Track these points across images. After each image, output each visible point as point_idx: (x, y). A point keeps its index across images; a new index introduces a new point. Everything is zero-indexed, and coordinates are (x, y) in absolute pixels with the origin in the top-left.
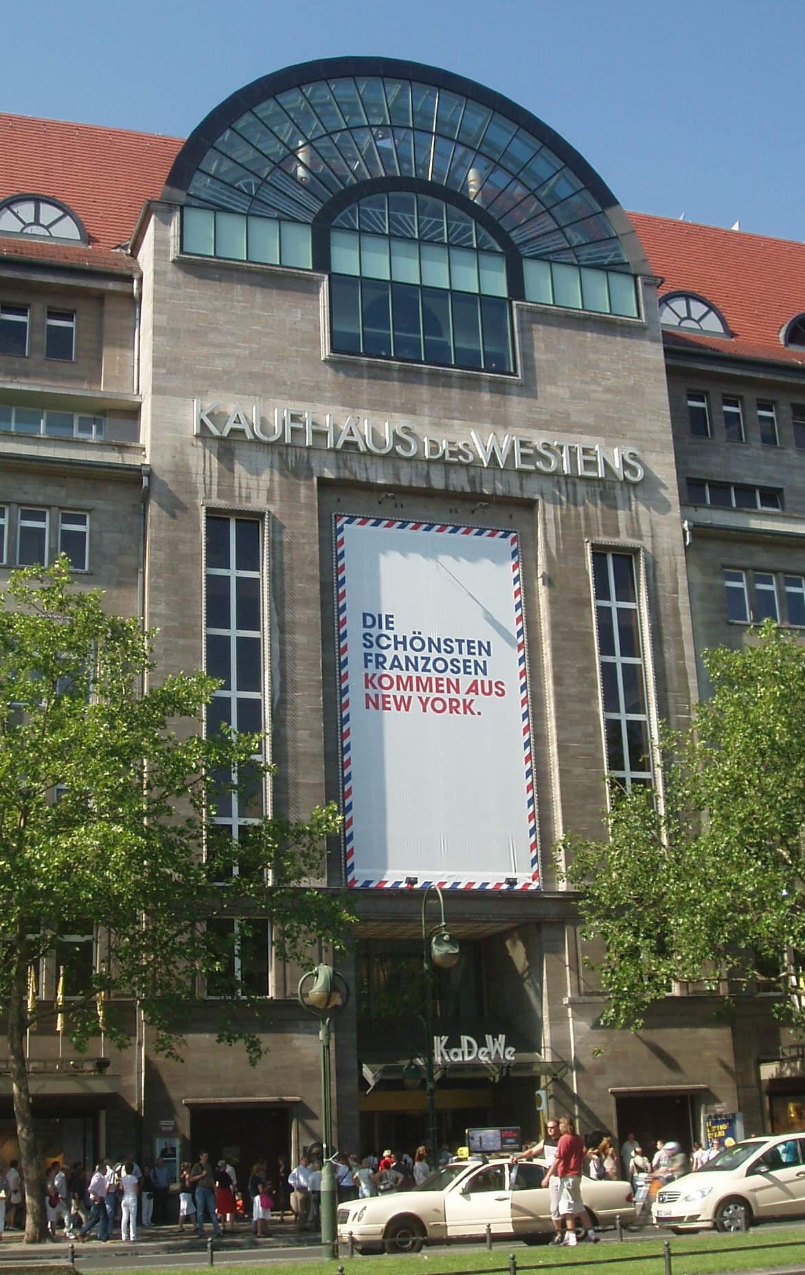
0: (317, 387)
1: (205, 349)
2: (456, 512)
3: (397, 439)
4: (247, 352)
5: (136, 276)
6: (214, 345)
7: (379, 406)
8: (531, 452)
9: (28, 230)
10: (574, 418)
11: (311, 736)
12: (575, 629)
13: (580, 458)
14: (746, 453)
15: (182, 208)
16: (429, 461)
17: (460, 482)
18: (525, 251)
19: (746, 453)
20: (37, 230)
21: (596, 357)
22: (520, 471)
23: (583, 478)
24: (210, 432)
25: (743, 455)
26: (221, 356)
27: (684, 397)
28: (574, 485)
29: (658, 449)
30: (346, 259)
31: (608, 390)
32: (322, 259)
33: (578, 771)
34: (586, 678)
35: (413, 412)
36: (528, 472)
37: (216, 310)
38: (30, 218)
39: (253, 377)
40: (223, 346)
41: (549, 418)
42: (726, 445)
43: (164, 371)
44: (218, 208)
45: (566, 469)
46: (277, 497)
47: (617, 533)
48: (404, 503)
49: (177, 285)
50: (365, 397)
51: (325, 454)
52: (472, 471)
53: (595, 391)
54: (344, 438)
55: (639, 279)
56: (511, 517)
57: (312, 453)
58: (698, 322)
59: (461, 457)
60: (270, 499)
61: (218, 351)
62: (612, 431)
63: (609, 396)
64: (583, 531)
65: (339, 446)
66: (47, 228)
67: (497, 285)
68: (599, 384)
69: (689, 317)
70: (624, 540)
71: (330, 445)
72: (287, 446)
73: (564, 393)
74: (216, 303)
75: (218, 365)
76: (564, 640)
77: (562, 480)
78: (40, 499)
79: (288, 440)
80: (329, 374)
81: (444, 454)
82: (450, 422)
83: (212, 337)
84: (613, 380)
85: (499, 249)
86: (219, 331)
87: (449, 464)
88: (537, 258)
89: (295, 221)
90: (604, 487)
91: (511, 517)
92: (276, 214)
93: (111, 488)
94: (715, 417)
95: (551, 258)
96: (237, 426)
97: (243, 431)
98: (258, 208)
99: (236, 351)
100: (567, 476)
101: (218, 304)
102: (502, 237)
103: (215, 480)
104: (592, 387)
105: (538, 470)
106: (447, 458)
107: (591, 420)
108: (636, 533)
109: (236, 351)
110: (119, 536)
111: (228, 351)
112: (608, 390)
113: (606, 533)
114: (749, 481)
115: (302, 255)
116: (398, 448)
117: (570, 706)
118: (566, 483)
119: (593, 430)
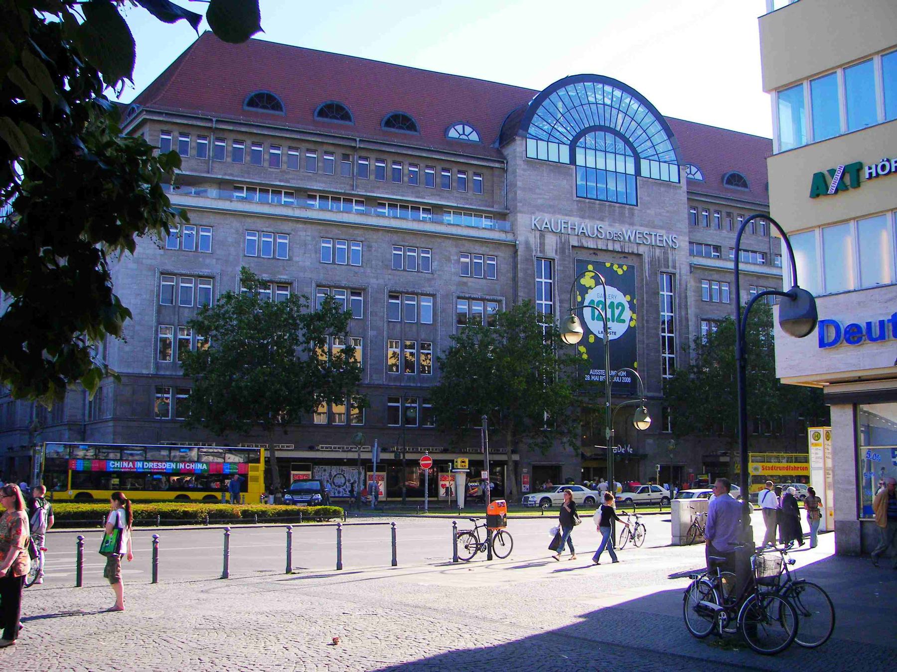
0: (571, 211)
5: (505, 162)
6: (538, 194)
7: (592, 218)
8: (641, 236)
9: (461, 137)
10: (656, 223)
13: (658, 238)
16: (608, 239)
18: (641, 155)
28: (655, 249)
35: (602, 220)
36: (640, 244)
38: (461, 132)
39: (551, 206)
44: (537, 139)
45: (653, 244)
46: (558, 253)
49: (524, 170)
50: (587, 214)
54: (581, 231)
58: (694, 175)
60: (556, 254)
61: (539, 196)
63: (668, 214)
66: (467, 136)
67: (631, 170)
69: (690, 173)
70: (670, 270)
75: (540, 202)
82: (614, 224)
83: (537, 191)
88: (644, 158)
89: (564, 144)
92: (557, 141)
94: (699, 217)
95: (650, 158)
96: (546, 226)
98: (551, 139)
102: (633, 149)
103: (539, 246)
107: (661, 224)
108: (674, 267)
112: (668, 212)
113: (665, 267)
114: (709, 243)
115: (565, 158)
116: (599, 235)
119: (662, 228)
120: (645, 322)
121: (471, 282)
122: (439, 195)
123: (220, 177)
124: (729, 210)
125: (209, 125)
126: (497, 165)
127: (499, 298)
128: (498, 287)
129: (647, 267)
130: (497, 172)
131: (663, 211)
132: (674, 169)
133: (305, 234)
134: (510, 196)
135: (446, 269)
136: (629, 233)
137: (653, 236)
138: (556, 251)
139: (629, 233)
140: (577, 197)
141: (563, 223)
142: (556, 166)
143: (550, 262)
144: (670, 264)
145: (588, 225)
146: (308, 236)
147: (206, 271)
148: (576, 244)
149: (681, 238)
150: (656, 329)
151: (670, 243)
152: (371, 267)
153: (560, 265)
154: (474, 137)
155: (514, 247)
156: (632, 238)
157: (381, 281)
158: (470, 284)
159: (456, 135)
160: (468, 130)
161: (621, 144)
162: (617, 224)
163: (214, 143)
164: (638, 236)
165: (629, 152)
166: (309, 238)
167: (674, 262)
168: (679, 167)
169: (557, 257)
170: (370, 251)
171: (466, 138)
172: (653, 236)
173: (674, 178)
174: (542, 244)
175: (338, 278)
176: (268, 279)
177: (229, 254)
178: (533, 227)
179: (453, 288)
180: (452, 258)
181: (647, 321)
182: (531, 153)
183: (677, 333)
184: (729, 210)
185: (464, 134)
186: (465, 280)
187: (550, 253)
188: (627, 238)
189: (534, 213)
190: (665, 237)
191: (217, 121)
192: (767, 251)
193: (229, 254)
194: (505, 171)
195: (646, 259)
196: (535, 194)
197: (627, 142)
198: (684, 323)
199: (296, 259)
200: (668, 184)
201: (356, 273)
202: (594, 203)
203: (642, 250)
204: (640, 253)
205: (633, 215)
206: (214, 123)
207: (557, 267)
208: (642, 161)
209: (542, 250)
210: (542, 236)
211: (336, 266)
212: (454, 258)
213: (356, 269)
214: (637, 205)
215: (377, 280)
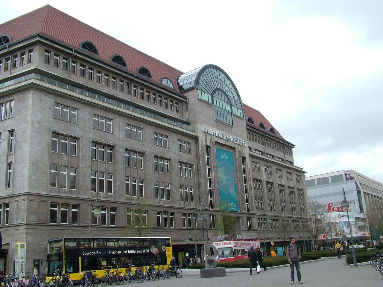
7: (220, 129)
17: (228, 144)
20: (167, 84)
31: (241, 130)
33: (242, 193)
35: (223, 131)
37: (202, 109)
38: (167, 83)
44: (202, 90)
47: (243, 154)
54: (218, 135)
57: (214, 137)
62: (242, 138)
63: (241, 131)
66: (169, 84)
70: (244, 156)
75: (204, 119)
80: (215, 123)
87: (227, 140)
92: (207, 92)
93: (192, 139)
95: (234, 106)
99: (205, 117)
102: (230, 101)
119: (240, 137)
120: (239, 178)
122: (164, 110)
123: (77, 82)
125: (71, 52)
126: (184, 100)
127: (193, 164)
129: (237, 153)
130: (184, 104)
132: (241, 112)
133: (119, 121)
134: (191, 115)
135: (174, 147)
142: (208, 103)
143: (208, 147)
144: (244, 153)
145: (219, 133)
146: (120, 121)
147: (75, 135)
148: (216, 141)
149: (246, 142)
152: (146, 142)
153: (213, 149)
154: (171, 86)
155: (196, 139)
157: (150, 150)
158: (182, 155)
159: (165, 84)
160: (169, 82)
161: (226, 98)
162: (227, 133)
163: (71, 63)
164: (234, 139)
165: (229, 102)
166: (121, 123)
167: (245, 152)
168: (243, 111)
169: (211, 146)
170: (145, 133)
171: (168, 85)
173: (242, 116)
174: (206, 139)
175: (133, 146)
176: (104, 143)
177: (86, 126)
178: (203, 131)
179: (177, 157)
180: (175, 142)
182: (200, 97)
183: (248, 184)
185: (168, 83)
186: (180, 153)
187: (209, 144)
189: (202, 124)
191: (75, 51)
192: (263, 151)
193: (86, 126)
194: (187, 103)
195: (236, 149)
197: (228, 98)
198: (250, 180)
199: (116, 133)
200: (240, 118)
201: (141, 144)
202: (220, 123)
203: (235, 146)
204: (235, 147)
205: (232, 130)
206: (74, 51)
208: (233, 107)
209: (206, 142)
210: (206, 136)
211: (132, 140)
212: (176, 142)
213: (141, 142)
214: (233, 126)
215: (149, 149)
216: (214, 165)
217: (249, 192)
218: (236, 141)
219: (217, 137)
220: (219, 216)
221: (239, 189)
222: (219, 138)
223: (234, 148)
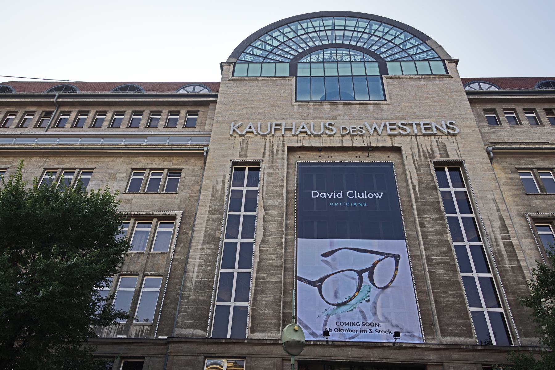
1: (239, 106)
2: (359, 157)
3: (326, 128)
4: (258, 106)
10: (418, 113)
11: (276, 257)
12: (429, 200)
13: (423, 127)
14: (522, 130)
15: (235, 63)
16: (343, 136)
17: (358, 142)
19: (522, 130)
21: (427, 90)
22: (390, 135)
23: (424, 135)
24: (237, 133)
25: (521, 131)
26: (246, 108)
27: (482, 112)
29: (466, 121)
30: (302, 71)
32: (293, 72)
34: (439, 223)
36: (395, 135)
40: (248, 104)
41: (404, 115)
42: (510, 128)
43: (220, 115)
48: (332, 155)
51: (292, 138)
52: (365, 138)
53: (427, 103)
54: (300, 129)
55: (445, 61)
56: (389, 157)
59: (358, 132)
61: (245, 107)
63: (436, 104)
64: (428, 157)
65: (298, 133)
68: (430, 100)
71: (293, 133)
72: (273, 136)
73: (413, 105)
74: (245, 91)
76: (422, 205)
77: (414, 138)
78: (160, 167)
79: (273, 133)
81: (350, 132)
84: (437, 97)
85: (374, 60)
86: (247, 100)
90: (439, 138)
91: (389, 157)
92: (275, 61)
95: (400, 60)
97: (252, 132)
99: (253, 106)
100: (416, 135)
101: (247, 92)
104: (426, 101)
105: (400, 134)
106: (351, 133)
109: (253, 106)
110: (194, 178)
111: (249, 106)
112: (435, 101)
117: (430, 237)
118: (416, 139)
121: (135, 198)
124: (547, 106)
127: (174, 213)
128: (177, 201)
131: (426, 101)
136: (375, 125)
137: (414, 125)
138: (264, 154)
139: (375, 125)
140: (296, 101)
141: (274, 125)
143: (255, 167)
150: (442, 235)
151: (445, 130)
156: (380, 131)
165: (368, 57)
168: (443, 61)
172: (414, 125)
178: (231, 132)
181: (422, 225)
184: (547, 106)
188: (372, 131)
190: (433, 125)
196: (241, 105)
207: (264, 168)
214: (385, 99)
216: (269, 203)
217: (495, 265)
218: (405, 130)
219: (297, 136)
220: (268, 362)
221: (425, 260)
222: (310, 135)
223: (398, 150)
